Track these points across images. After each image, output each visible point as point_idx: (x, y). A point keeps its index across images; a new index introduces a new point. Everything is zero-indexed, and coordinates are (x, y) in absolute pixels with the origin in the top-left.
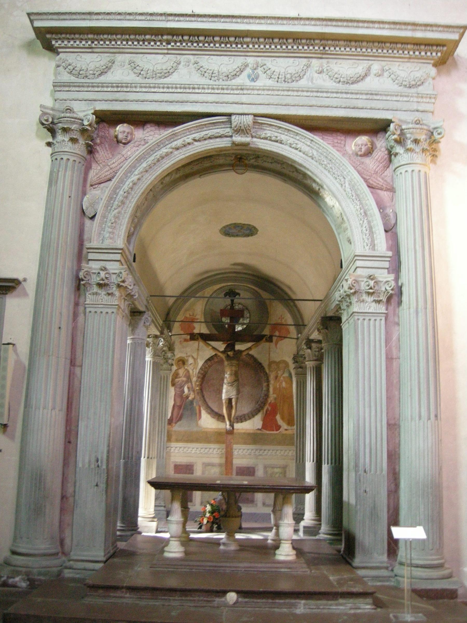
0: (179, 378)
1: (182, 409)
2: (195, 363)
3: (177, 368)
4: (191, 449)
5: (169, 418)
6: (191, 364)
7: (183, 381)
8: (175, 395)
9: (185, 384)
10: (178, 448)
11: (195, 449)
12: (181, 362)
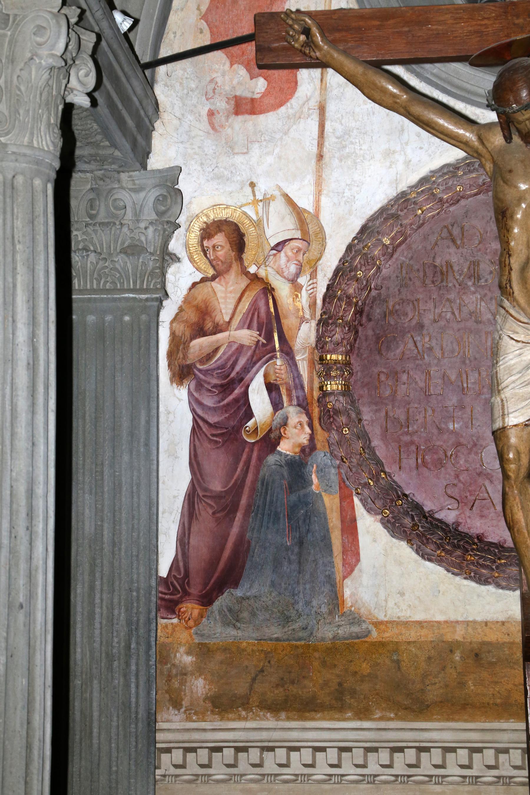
0: (217, 329)
1: (239, 516)
2: (305, 238)
3: (198, 276)
4: (307, 755)
5: (163, 572)
6: (279, 246)
7: (241, 348)
8: (196, 430)
9: (252, 363)
10: (229, 753)
11: (332, 755)
12: (220, 239)
